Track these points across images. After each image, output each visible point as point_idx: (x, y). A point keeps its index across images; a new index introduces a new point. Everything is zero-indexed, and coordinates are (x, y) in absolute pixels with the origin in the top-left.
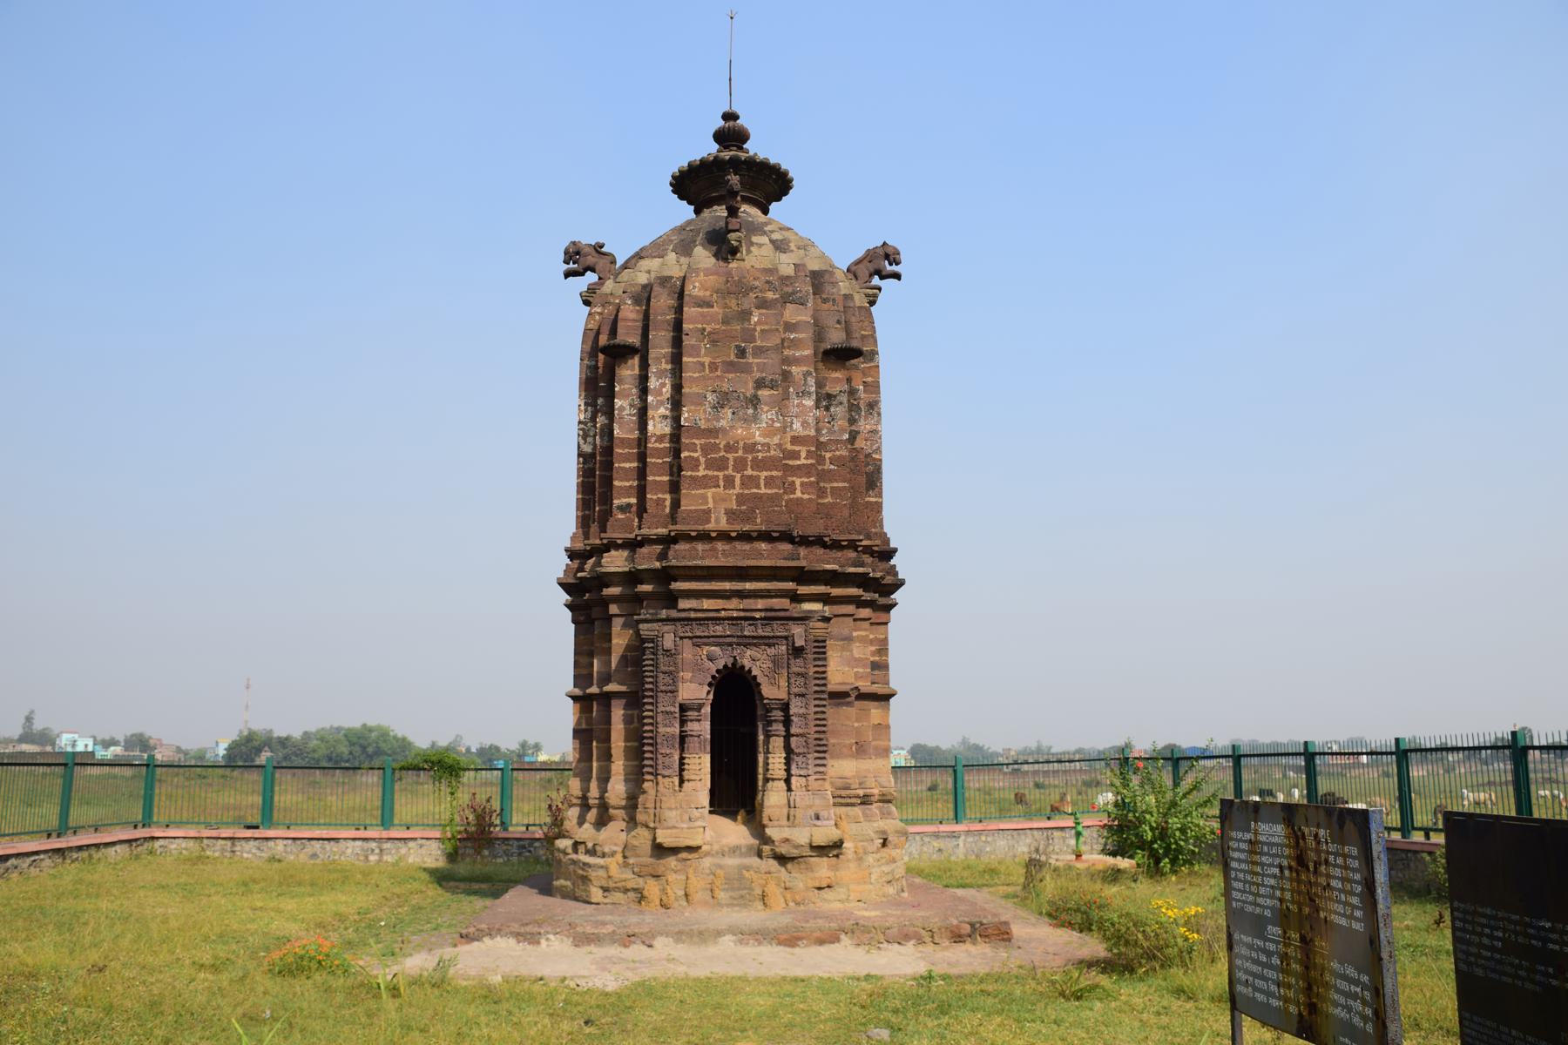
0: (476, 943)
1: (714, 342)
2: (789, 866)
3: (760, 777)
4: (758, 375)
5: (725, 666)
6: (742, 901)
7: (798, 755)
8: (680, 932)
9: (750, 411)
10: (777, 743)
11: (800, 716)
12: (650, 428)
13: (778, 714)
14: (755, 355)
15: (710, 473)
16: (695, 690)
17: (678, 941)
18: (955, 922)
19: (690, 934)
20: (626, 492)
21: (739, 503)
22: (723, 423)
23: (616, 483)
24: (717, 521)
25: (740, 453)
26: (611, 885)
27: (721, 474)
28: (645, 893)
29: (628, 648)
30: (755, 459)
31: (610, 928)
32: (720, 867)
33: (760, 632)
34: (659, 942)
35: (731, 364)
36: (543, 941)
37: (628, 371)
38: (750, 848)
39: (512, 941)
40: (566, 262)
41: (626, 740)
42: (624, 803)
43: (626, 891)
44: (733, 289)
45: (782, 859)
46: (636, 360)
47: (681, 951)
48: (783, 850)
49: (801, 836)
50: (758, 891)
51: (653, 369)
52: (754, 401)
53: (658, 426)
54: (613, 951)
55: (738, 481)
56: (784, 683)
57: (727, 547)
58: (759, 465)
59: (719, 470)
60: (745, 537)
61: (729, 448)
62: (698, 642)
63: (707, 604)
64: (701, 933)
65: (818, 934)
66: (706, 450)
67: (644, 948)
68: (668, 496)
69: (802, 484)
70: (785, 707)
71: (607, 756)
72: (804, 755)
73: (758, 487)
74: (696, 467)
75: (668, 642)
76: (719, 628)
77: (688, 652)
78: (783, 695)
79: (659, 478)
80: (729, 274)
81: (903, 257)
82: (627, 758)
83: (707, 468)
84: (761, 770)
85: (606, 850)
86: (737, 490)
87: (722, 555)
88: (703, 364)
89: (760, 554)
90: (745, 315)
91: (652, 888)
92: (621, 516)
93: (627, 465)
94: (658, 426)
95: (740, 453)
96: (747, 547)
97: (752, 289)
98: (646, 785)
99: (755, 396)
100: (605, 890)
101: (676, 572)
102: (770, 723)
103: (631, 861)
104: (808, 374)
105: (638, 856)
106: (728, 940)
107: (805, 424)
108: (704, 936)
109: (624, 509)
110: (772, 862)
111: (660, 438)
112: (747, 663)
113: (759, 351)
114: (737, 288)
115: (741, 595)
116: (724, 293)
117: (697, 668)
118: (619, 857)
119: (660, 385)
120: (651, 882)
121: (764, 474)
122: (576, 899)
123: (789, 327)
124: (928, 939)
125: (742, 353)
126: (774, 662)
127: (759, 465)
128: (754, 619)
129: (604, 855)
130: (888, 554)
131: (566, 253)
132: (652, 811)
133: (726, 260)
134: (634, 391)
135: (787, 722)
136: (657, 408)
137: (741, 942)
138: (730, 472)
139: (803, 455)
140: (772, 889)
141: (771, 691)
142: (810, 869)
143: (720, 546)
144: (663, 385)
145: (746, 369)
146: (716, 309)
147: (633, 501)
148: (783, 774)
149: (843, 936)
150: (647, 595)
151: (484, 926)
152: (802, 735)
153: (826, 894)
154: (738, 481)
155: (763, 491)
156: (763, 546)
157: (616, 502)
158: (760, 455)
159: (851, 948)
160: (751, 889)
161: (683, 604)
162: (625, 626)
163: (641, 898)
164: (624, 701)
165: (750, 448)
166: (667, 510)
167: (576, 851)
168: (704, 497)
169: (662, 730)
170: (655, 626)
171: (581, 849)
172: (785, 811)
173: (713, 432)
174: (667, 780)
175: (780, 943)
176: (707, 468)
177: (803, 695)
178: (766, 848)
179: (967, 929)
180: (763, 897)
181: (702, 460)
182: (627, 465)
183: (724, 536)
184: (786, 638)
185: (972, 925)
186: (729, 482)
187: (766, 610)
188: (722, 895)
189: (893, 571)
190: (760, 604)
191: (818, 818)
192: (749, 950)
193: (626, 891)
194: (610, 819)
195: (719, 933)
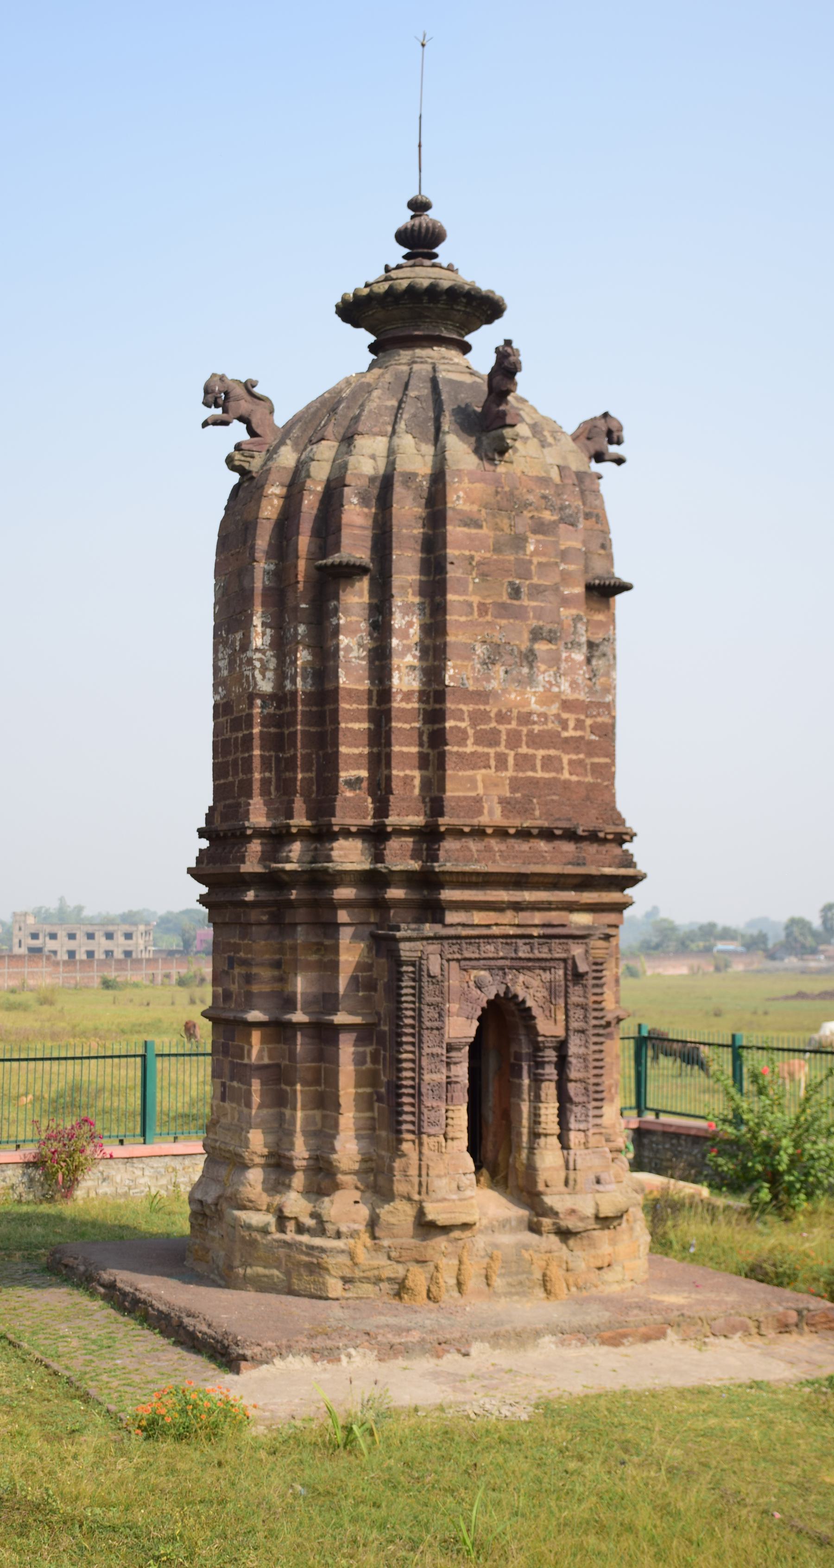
0: (265, 1366)
1: (483, 575)
2: (571, 1242)
3: (525, 1131)
4: (534, 623)
5: (497, 995)
6: (520, 1289)
8: (496, 1335)
9: (525, 670)
10: (549, 1090)
11: (579, 1057)
12: (395, 681)
13: (551, 1055)
14: (531, 596)
15: (480, 749)
16: (462, 1027)
17: (495, 1346)
18: (781, 1309)
19: (507, 1337)
20: (355, 762)
21: (513, 790)
22: (494, 685)
23: (343, 749)
24: (491, 812)
25: (514, 725)
26: (358, 1274)
27: (491, 751)
28: (409, 1283)
29: (361, 966)
30: (530, 733)
31: (415, 1336)
32: (496, 1246)
33: (537, 954)
34: (476, 1349)
35: (503, 606)
36: (344, 1358)
37: (356, 598)
38: (520, 1220)
39: (307, 1360)
40: (207, 404)
41: (358, 1085)
42: (356, 1166)
43: (378, 1280)
44: (504, 504)
45: (565, 1234)
46: (364, 585)
47: (502, 1358)
48: (570, 1223)
49: (586, 1205)
50: (538, 1275)
51: (397, 602)
52: (530, 658)
53: (405, 678)
54: (427, 1363)
55: (511, 761)
56: (561, 1017)
57: (503, 847)
58: (535, 740)
59: (490, 745)
60: (524, 834)
61: (502, 718)
63: (478, 917)
64: (518, 1335)
65: (643, 1329)
66: (477, 718)
67: (458, 1357)
68: (417, 774)
69: (571, 762)
70: (562, 1047)
71: (326, 1102)
72: (584, 1105)
73: (534, 769)
74: (463, 742)
75: (434, 965)
76: (491, 948)
77: (455, 979)
78: (560, 1032)
79: (405, 749)
80: (497, 482)
81: (626, 434)
82: (358, 1109)
83: (476, 743)
84: (525, 1122)
85: (344, 1229)
86: (510, 773)
87: (498, 858)
88: (470, 605)
89: (541, 858)
90: (519, 542)
91: (418, 1278)
92: (349, 794)
93: (356, 726)
94: (405, 678)
95: (514, 725)
96: (524, 846)
97: (527, 505)
98: (406, 1147)
99: (531, 651)
100: (346, 1280)
101: (448, 878)
102: (540, 1065)
103: (386, 1243)
104: (577, 619)
105: (394, 1236)
106: (547, 1341)
107: (574, 685)
108: (522, 1337)
109: (353, 784)
110: (554, 1239)
111: (407, 696)
112: (521, 993)
113: (537, 591)
114: (507, 503)
115: (517, 907)
116: (497, 509)
117: (464, 996)
118: (366, 1238)
119: (406, 624)
120: (415, 1269)
121: (541, 753)
122: (320, 1298)
123: (564, 555)
124: (754, 1331)
125: (516, 592)
127: (535, 740)
128: (531, 937)
129: (338, 1235)
130: (622, 838)
131: (207, 391)
132: (416, 1180)
133: (491, 460)
134: (363, 625)
135: (562, 1063)
136: (403, 655)
137: (562, 1343)
138: (502, 749)
139: (571, 724)
140: (556, 1273)
141: (548, 1027)
142: (593, 1245)
143: (494, 843)
144: (410, 624)
145: (519, 614)
146: (485, 531)
147: (364, 774)
148: (555, 1129)
149: (669, 1331)
150: (397, 903)
151: (270, 1344)
153: (608, 1275)
154: (511, 761)
155: (540, 774)
156: (543, 845)
157: (344, 775)
158: (537, 728)
159: (677, 1344)
160: (530, 1273)
161: (451, 917)
162: (355, 937)
163: (401, 1289)
164: (354, 1035)
165: (525, 718)
166: (417, 791)
167: (282, 1229)
168: (473, 780)
169: (427, 1077)
170: (418, 945)
171: (291, 1226)
172: (563, 1174)
173: (483, 696)
174: (432, 1139)
175: (603, 1343)
176: (476, 743)
177: (583, 1031)
178: (547, 1222)
179: (793, 1317)
180: (545, 1282)
181: (471, 732)
182: (356, 726)
183: (501, 833)
184: (565, 960)
185: (799, 1312)
186: (501, 762)
187: (544, 926)
188: (498, 1282)
189: (628, 861)
190: (538, 918)
191: (598, 1182)
192: (576, 1353)
193: (378, 1280)
194: (337, 1187)
195: (537, 1334)
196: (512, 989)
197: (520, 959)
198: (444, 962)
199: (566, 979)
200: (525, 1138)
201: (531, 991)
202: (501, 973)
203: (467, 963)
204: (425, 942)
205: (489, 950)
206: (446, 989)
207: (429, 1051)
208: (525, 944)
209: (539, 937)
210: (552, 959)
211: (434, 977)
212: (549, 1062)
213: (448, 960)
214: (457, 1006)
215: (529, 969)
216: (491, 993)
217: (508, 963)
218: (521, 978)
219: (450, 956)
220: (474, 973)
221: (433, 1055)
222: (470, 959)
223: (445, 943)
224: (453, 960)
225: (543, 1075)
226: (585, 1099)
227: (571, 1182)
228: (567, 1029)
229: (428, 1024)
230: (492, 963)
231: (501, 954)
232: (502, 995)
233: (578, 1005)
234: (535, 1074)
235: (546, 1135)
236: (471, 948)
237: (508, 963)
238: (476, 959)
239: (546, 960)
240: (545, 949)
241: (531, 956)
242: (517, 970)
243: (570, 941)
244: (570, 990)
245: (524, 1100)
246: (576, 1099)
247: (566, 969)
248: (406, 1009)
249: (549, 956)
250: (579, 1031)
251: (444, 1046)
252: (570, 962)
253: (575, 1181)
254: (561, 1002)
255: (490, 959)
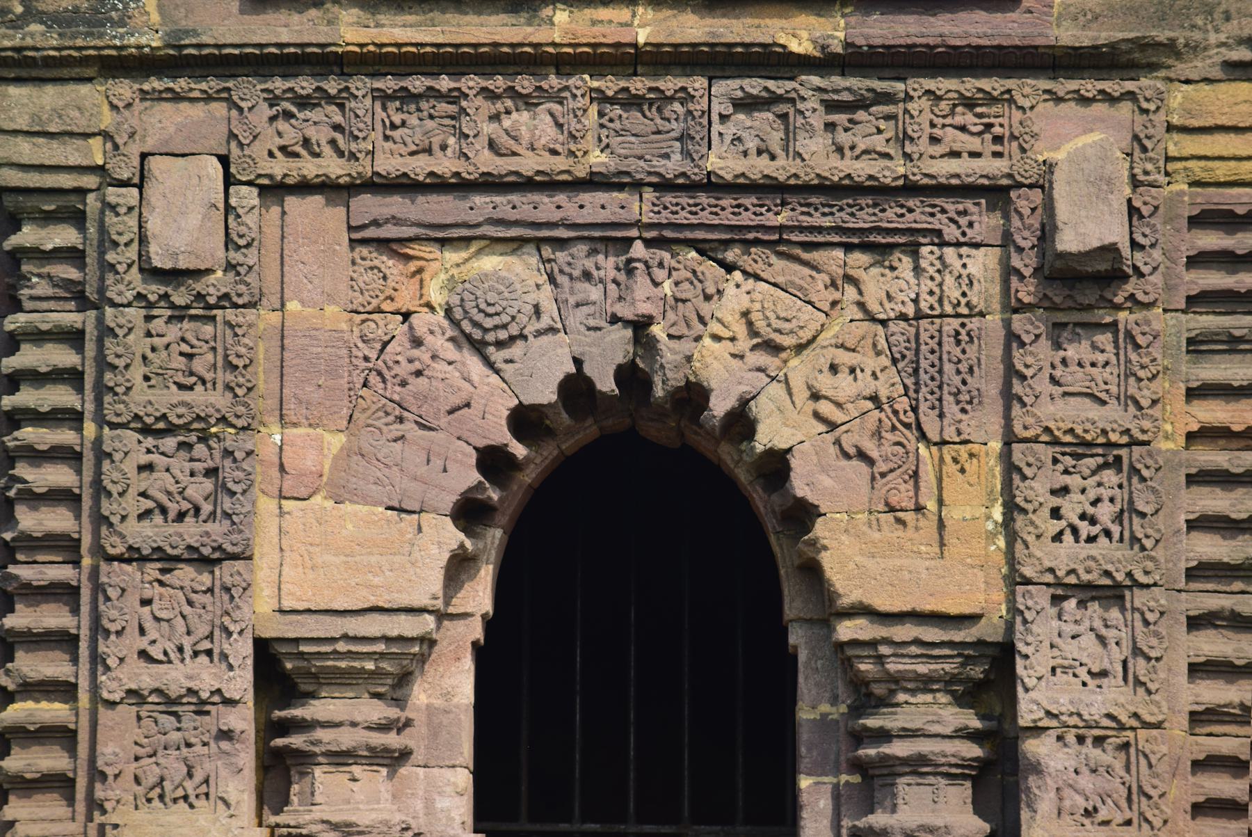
5: (576, 388)
11: (1091, 734)
13: (934, 723)
33: (818, 156)
56: (973, 504)
62: (387, 213)
70: (989, 674)
75: (181, 215)
78: (965, 583)
112: (724, 375)
117: (382, 392)
126: (907, 361)
141: (891, 554)
170: (89, 101)
177: (1111, 593)
184: (996, 194)
196: (670, 353)
197: (713, 185)
198: (246, 197)
199: (1014, 307)
201: (799, 369)
202: (608, 265)
203: (395, 205)
204: (124, 89)
205: (532, 135)
206: (264, 353)
207: (146, 678)
208: (747, 104)
209: (826, 63)
210: (910, 189)
211: (175, 276)
212: (917, 766)
213: (274, 190)
214: (336, 441)
215: (779, 242)
216: (540, 376)
217: (640, 207)
218: (736, 296)
219: (279, 168)
220: (443, 271)
221: (170, 703)
222: (405, 186)
223: (249, 90)
224: (305, 187)
228: (1015, 580)
229: (146, 534)
230: (546, 207)
231: (598, 159)
232: (606, 384)
236: (417, 126)
237: (640, 207)
238: (438, 185)
239: (878, 191)
240: (869, 132)
241: (781, 168)
242: (703, 249)
243: (1028, 88)
244: (1038, 356)
248: (36, 456)
249: (893, 170)
250: (1088, 592)
251: (242, 650)
252: (1024, 201)
254: (985, 427)
255: (527, 184)
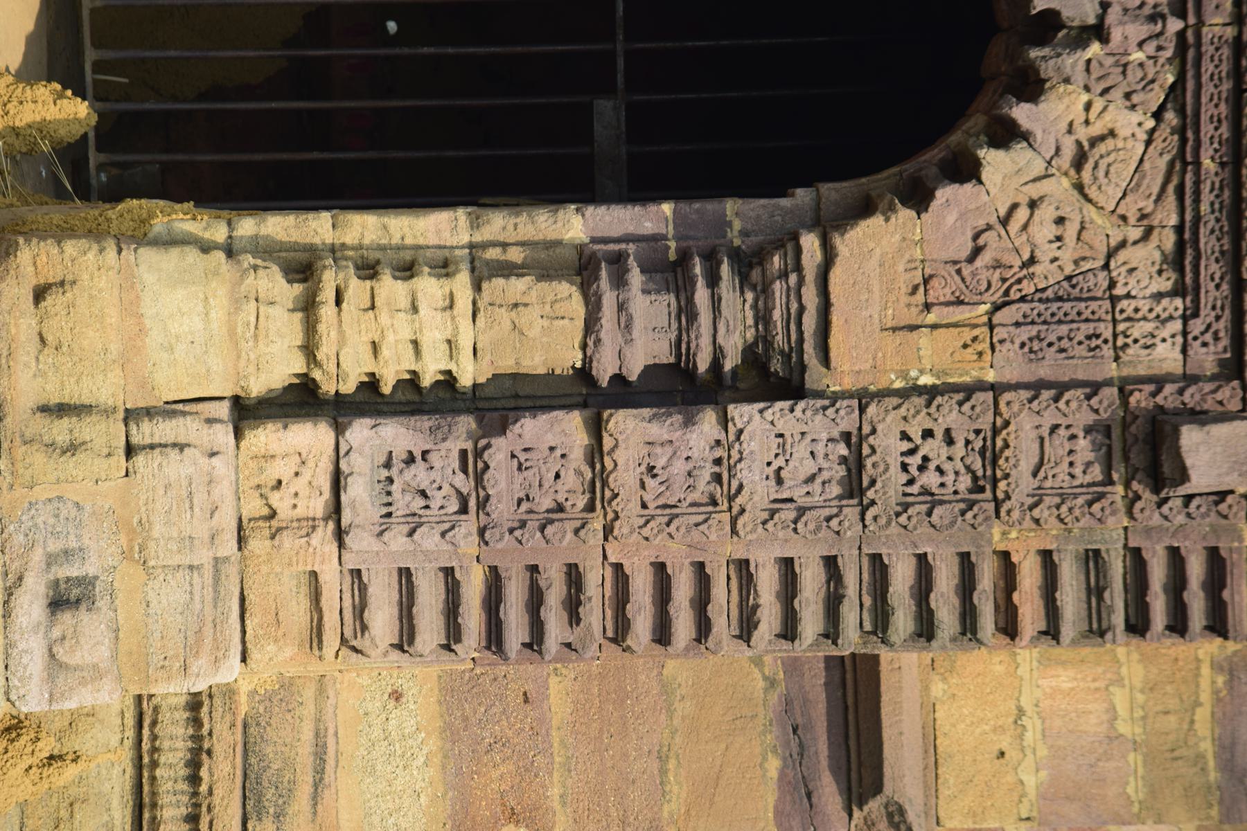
3: (317, 227)
7: (473, 463)
10: (542, 330)
56: (933, 357)
70: (774, 376)
84: (365, 228)
102: (671, 273)
112: (1053, 116)
126: (1070, 291)
135: (679, 387)
148: (344, 370)
152: (598, 487)
172: (106, 388)
177: (855, 486)
191: (59, 603)
196: (1073, 62)
199: (1125, 388)
200: (280, 226)
201: (1059, 187)
212: (687, 312)
218: (1130, 123)
225: (620, 281)
226: (502, 509)
227: (61, 430)
228: (863, 398)
233: (992, 456)
234: (618, 261)
235: (308, 307)
242: (1176, 90)
245: (475, 225)
246: (499, 451)
247: (1189, 379)
250: (855, 466)
253: (72, 448)
254: (1007, 365)
